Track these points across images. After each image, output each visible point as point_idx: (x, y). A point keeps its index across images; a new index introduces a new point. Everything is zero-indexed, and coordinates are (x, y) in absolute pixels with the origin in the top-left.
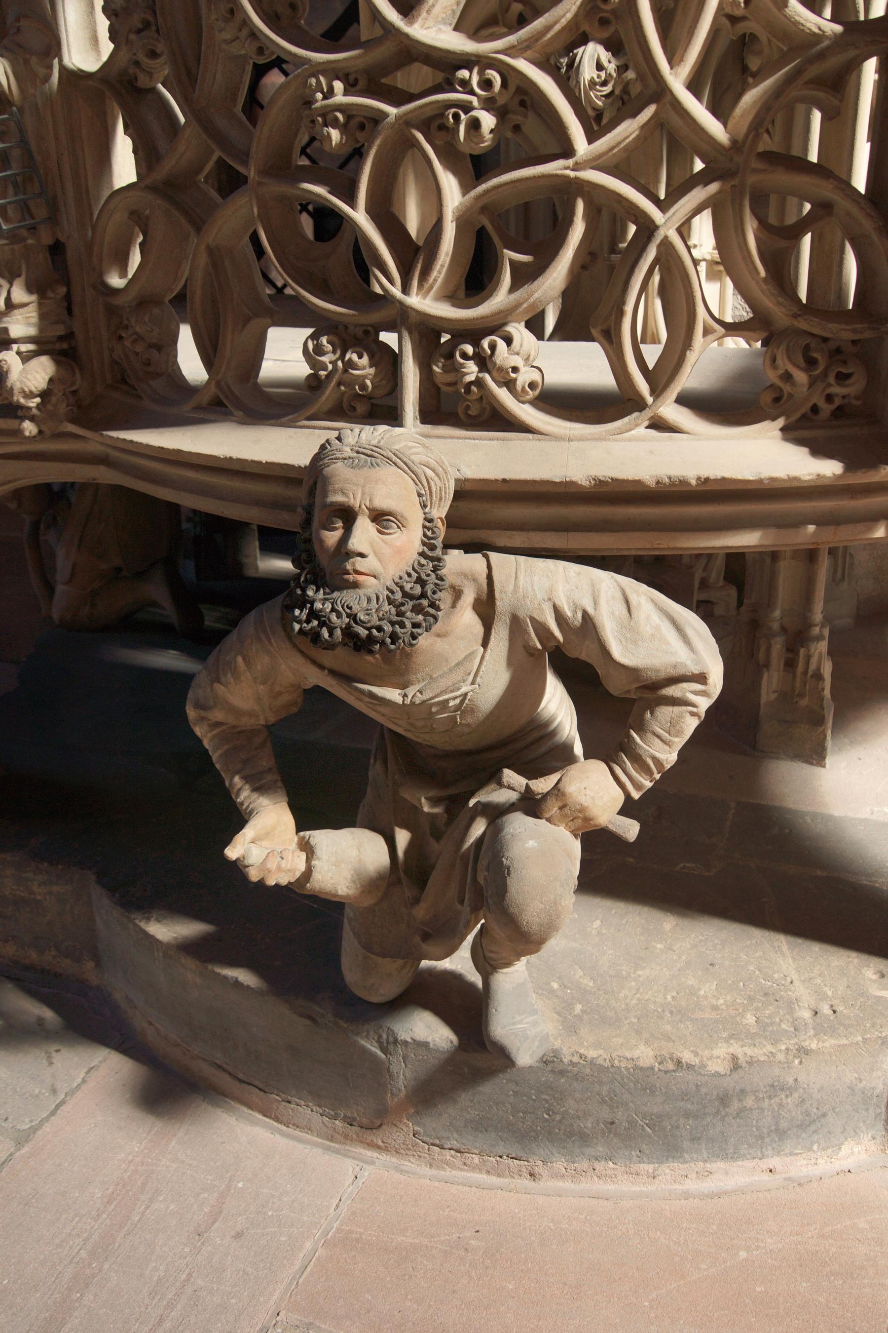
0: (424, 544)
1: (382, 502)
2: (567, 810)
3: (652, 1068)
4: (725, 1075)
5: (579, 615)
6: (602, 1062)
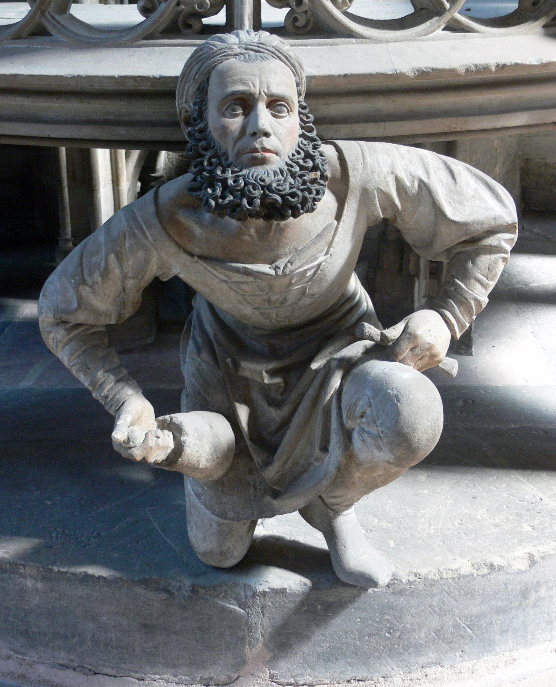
0: (302, 128)
1: (277, 90)
2: (418, 350)
4: (526, 571)
5: (416, 184)
6: (433, 577)
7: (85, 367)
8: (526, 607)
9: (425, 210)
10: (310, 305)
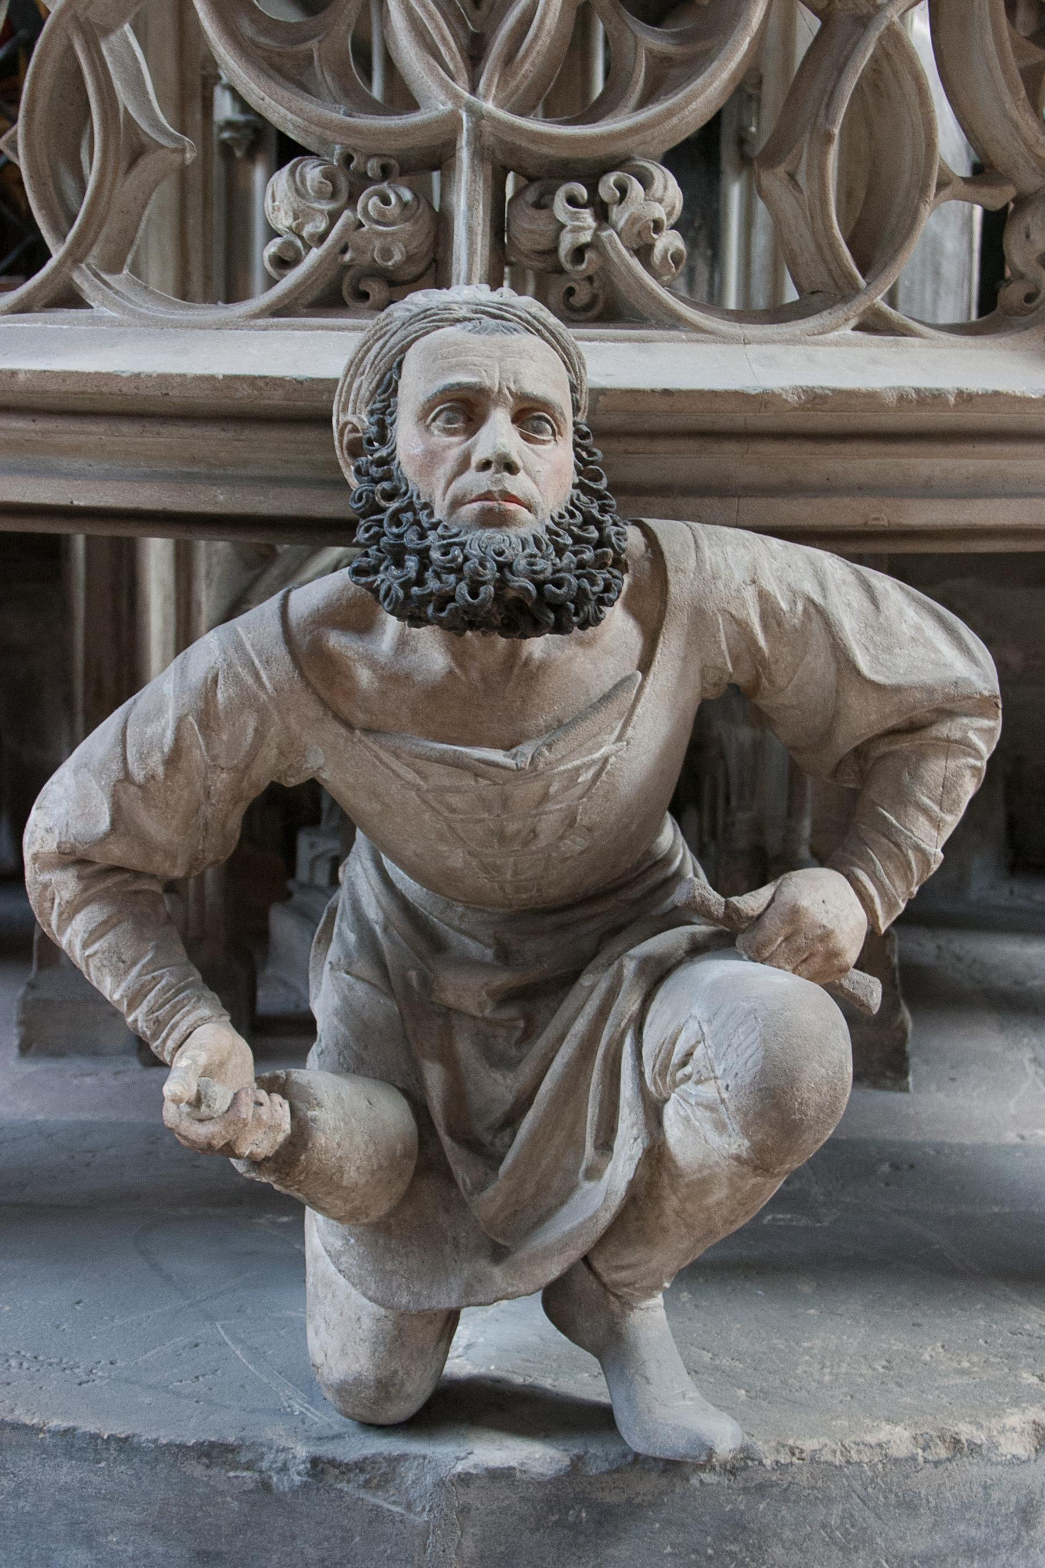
0: (579, 473)
2: (801, 941)
3: (914, 1458)
4: (1029, 1460)
5: (800, 607)
6: (829, 1457)
7: (115, 959)
8: (1031, 1546)
9: (818, 662)
10: (582, 853)
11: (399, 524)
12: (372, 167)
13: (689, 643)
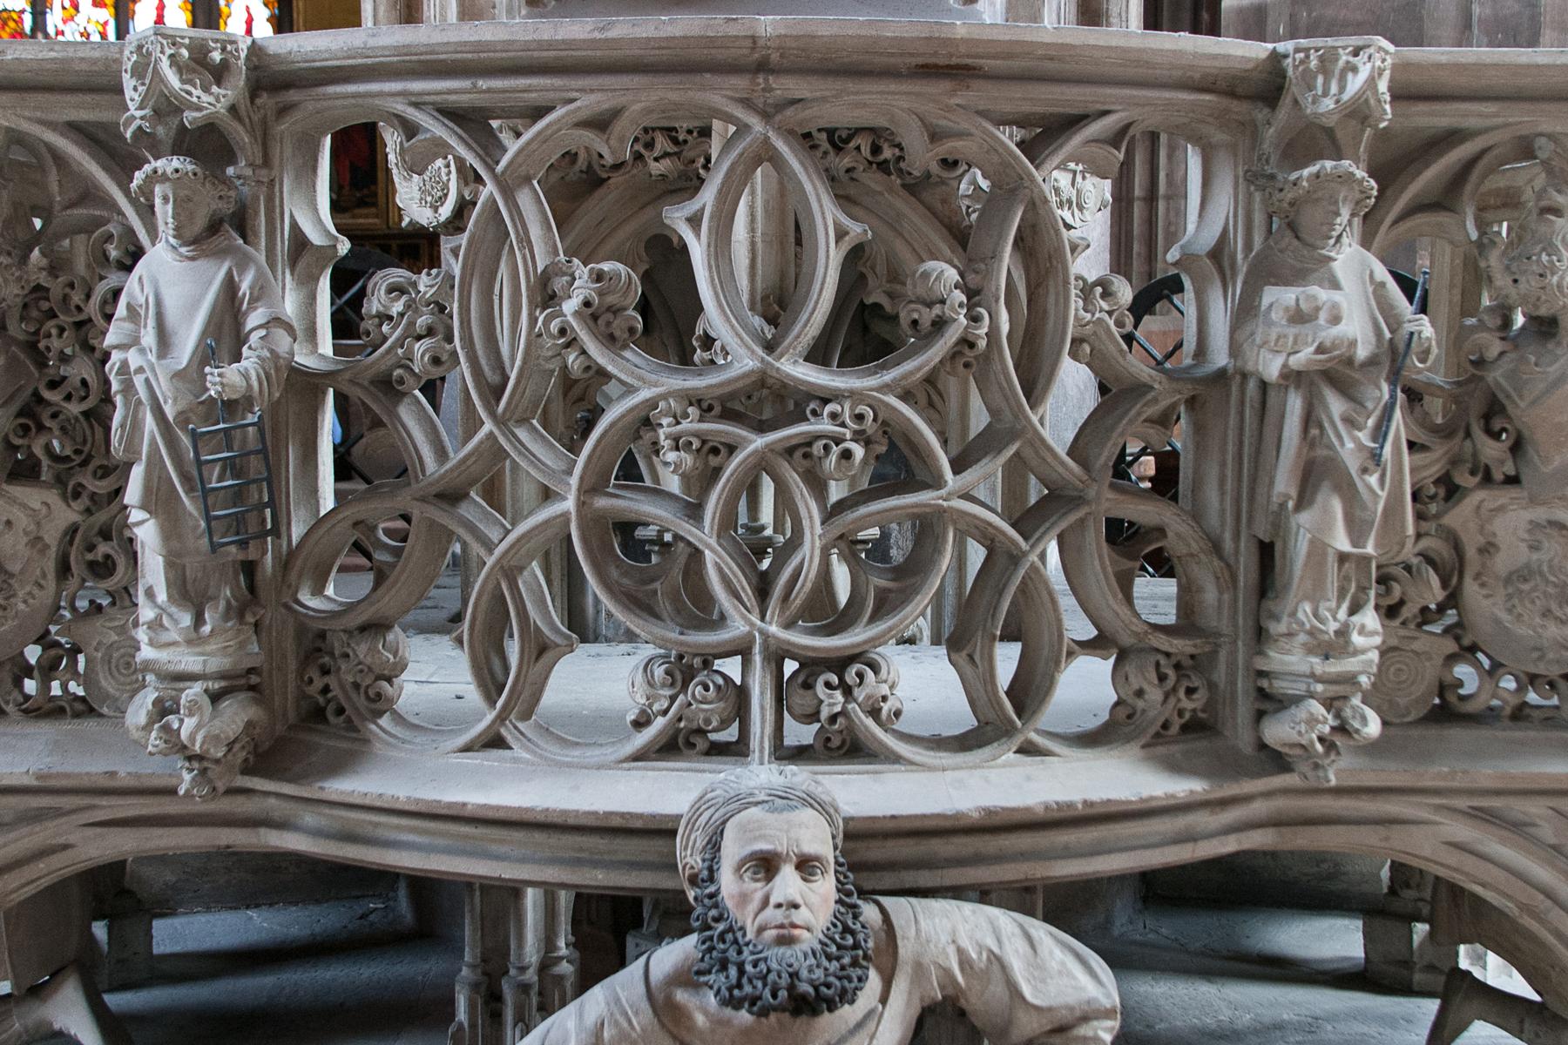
0: (839, 890)
5: (985, 956)
9: (998, 989)
11: (724, 942)
12: (697, 662)
13: (912, 982)
